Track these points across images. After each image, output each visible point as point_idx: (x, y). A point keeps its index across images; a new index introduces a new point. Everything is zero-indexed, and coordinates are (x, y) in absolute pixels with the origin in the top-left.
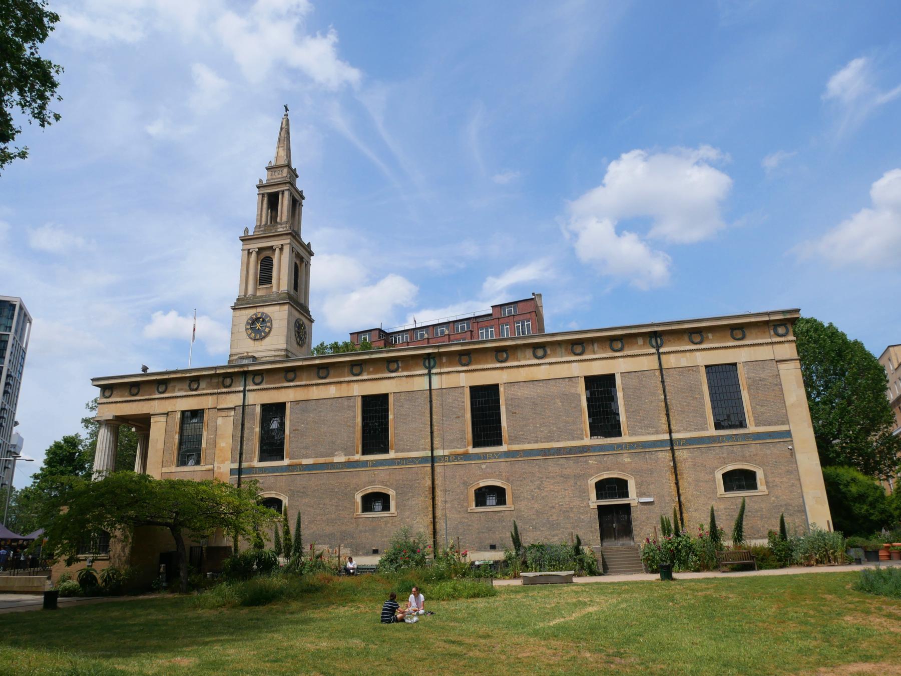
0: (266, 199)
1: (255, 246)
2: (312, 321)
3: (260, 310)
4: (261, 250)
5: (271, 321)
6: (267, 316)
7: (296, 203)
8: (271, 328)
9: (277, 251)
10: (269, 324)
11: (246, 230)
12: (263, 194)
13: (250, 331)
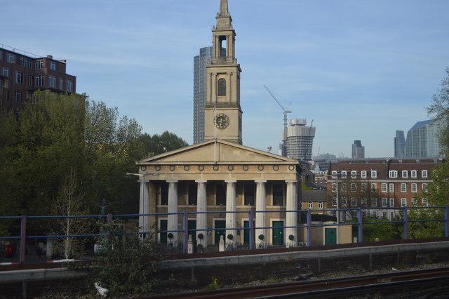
0: (217, 39)
3: (221, 112)
4: (218, 74)
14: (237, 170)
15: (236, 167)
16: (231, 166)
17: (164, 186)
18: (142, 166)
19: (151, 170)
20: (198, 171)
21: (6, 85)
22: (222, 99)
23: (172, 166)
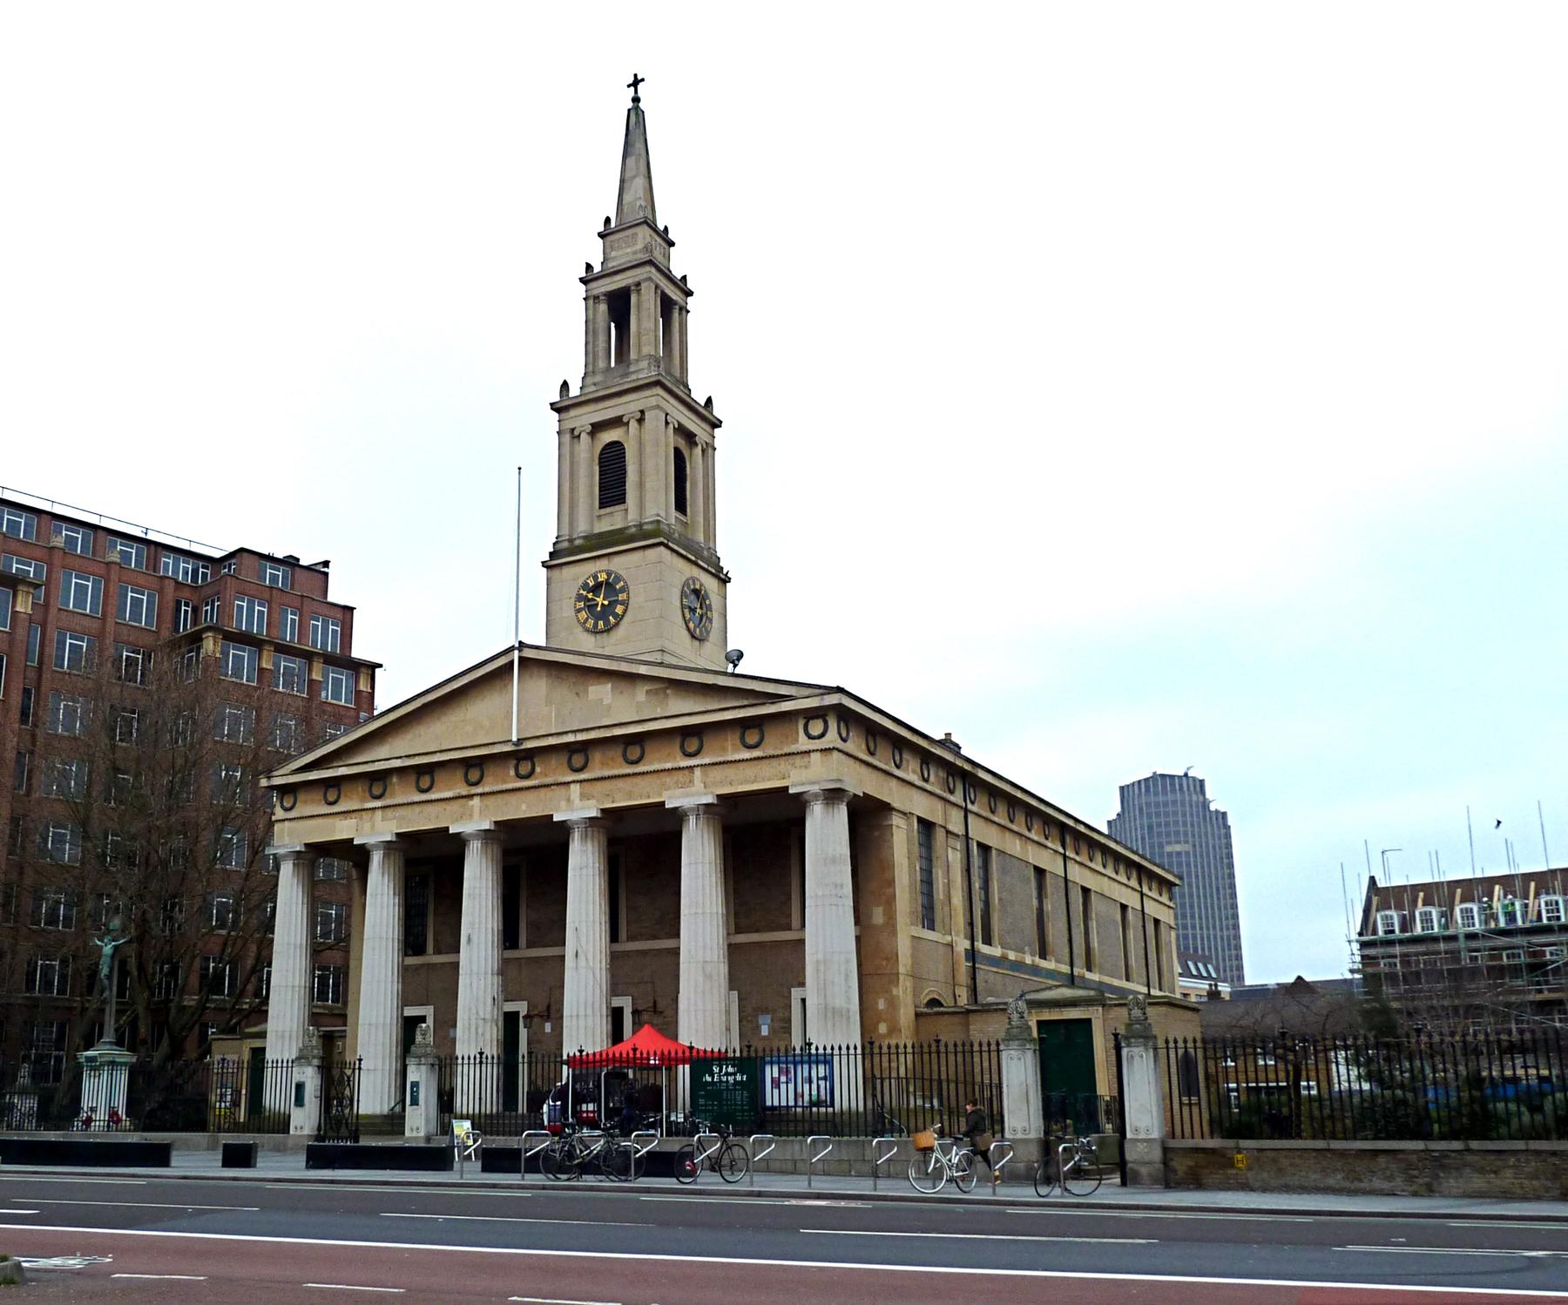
0: (603, 307)
1: (584, 418)
2: (725, 580)
4: (597, 428)
5: (624, 589)
6: (618, 578)
7: (672, 307)
8: (626, 604)
9: (633, 424)
10: (622, 597)
11: (565, 385)
12: (596, 298)
13: (583, 615)
14: (603, 764)
15: (597, 756)
16: (578, 752)
17: (358, 856)
18: (285, 790)
19: (309, 806)
20: (464, 790)
21: (24, 605)
22: (613, 520)
23: (377, 781)
